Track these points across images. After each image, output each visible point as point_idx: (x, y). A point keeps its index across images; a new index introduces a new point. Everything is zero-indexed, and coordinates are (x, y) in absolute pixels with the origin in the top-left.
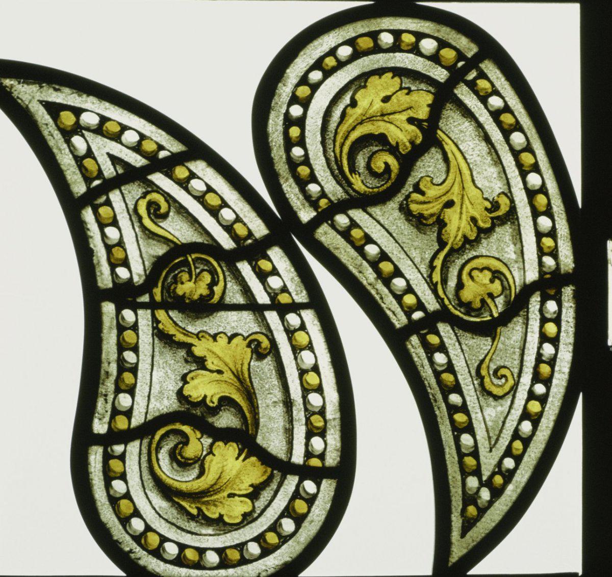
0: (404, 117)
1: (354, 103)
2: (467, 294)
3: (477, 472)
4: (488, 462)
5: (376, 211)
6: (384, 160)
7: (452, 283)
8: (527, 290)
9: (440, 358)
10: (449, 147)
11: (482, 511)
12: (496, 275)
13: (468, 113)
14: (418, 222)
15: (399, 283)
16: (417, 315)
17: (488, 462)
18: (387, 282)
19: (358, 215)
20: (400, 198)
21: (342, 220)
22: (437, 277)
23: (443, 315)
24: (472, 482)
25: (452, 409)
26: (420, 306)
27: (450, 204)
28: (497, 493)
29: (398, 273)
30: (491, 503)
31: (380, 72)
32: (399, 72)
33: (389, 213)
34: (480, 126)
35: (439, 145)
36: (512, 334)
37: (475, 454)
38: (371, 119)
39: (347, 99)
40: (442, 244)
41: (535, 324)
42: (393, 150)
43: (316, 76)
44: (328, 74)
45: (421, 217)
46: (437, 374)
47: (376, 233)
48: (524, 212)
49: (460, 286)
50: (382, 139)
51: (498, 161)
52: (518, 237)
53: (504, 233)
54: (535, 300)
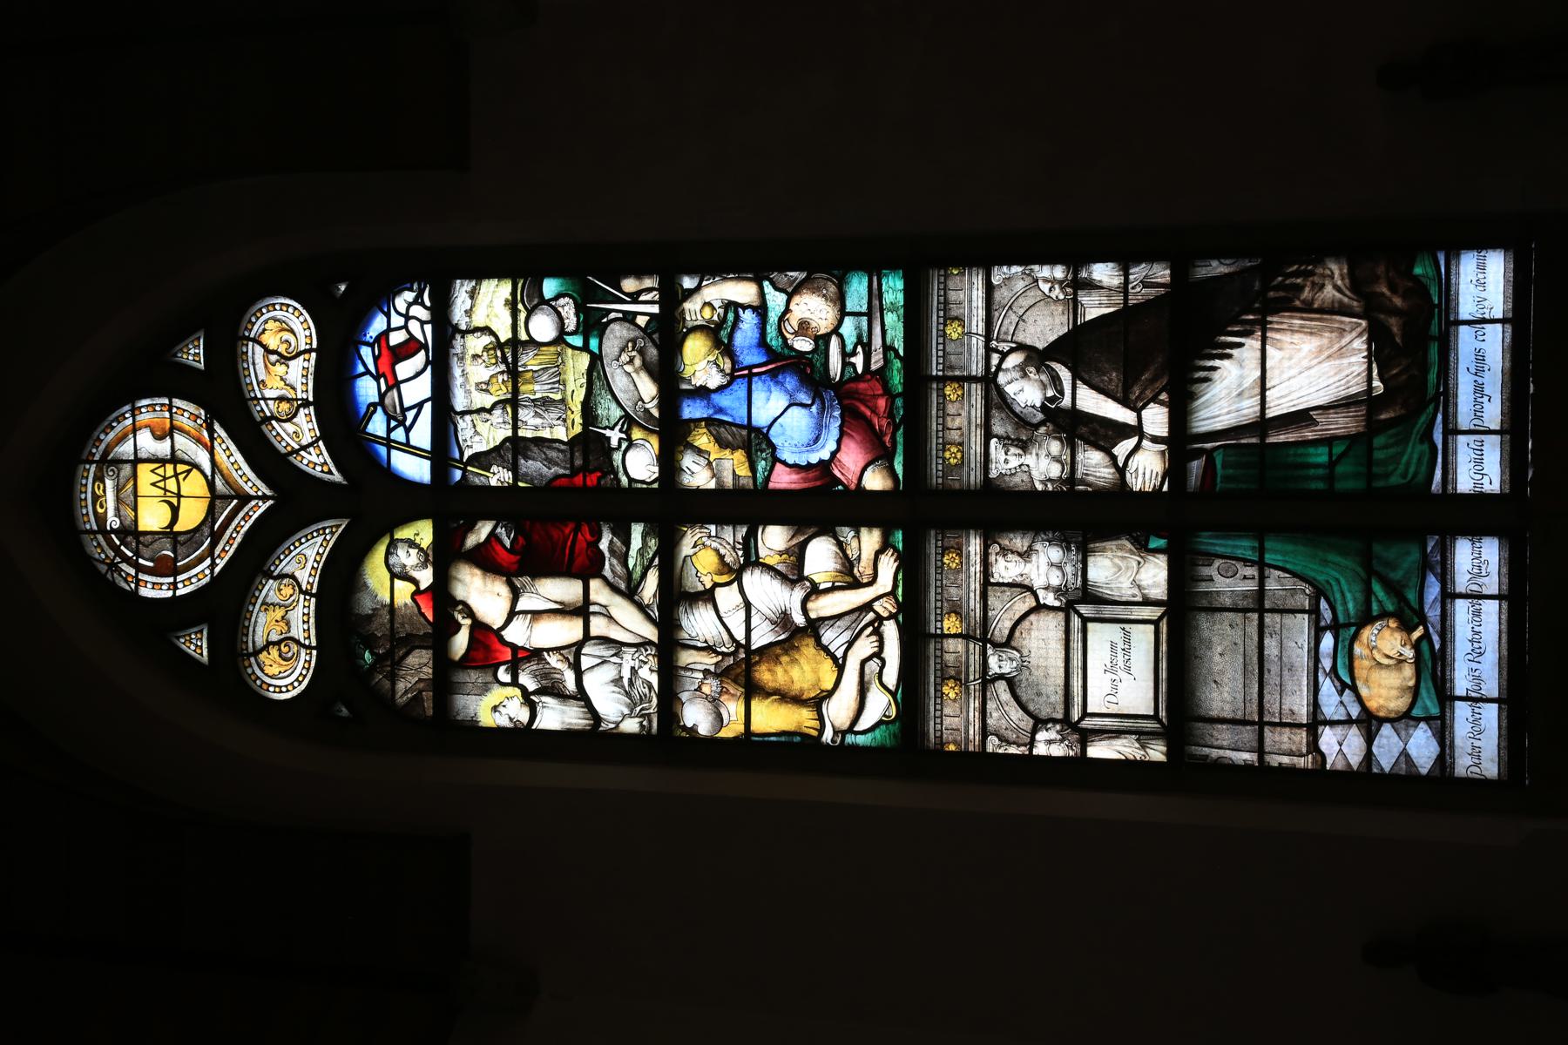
0: (270, 657)
1: (280, 672)
2: (291, 591)
3: (325, 539)
4: (320, 539)
5: (297, 637)
6: (284, 649)
7: (292, 598)
8: (275, 578)
9: (311, 581)
10: (265, 637)
11: (331, 527)
12: (280, 590)
13: (254, 642)
14: (288, 624)
15: (306, 611)
16: (308, 597)
17: (320, 539)
18: (309, 614)
19: (302, 640)
20: (288, 635)
21: (307, 643)
22: (295, 604)
23: (301, 591)
24: (328, 537)
25: (318, 563)
26: (305, 599)
27: (277, 621)
28: (324, 529)
29: (304, 614)
30: (328, 527)
31: (267, 675)
32: (262, 671)
33: (293, 633)
34: (253, 636)
35: (267, 640)
36: (288, 570)
37: (322, 545)
38: (279, 664)
39: (281, 675)
40: (287, 611)
41: (280, 567)
42: (280, 650)
43: (284, 689)
44: (280, 687)
45: (287, 625)
46: (315, 576)
47: (301, 631)
48: (260, 601)
49: (291, 596)
50: (280, 656)
51: (256, 622)
52: (267, 595)
53: (269, 600)
54: (275, 574)
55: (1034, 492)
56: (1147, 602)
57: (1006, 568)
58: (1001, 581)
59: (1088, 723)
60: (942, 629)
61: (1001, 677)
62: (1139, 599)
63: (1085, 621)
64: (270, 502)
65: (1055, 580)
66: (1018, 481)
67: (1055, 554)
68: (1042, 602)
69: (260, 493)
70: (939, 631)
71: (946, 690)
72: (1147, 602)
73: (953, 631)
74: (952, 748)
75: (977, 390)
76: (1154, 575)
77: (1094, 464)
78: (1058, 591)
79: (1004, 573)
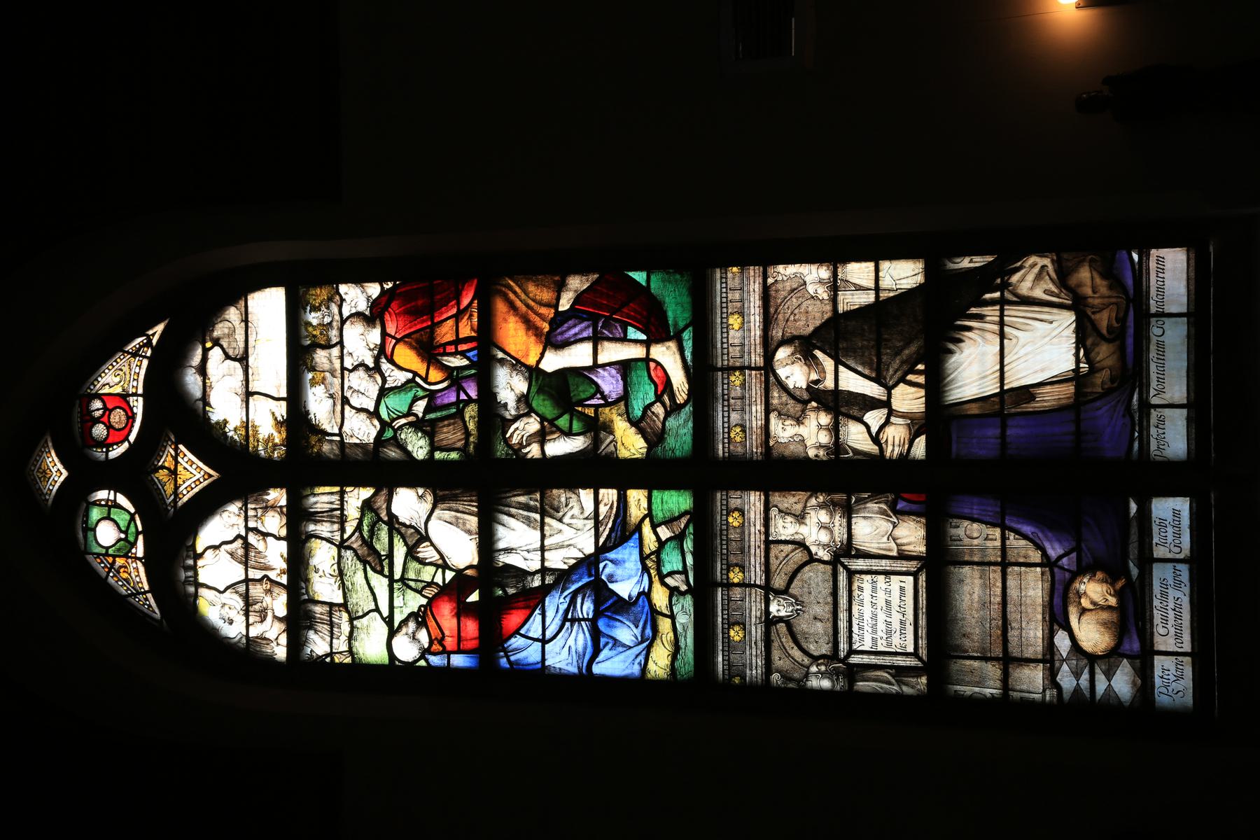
55: (807, 459)
56: (902, 556)
58: (780, 538)
59: (855, 659)
60: (728, 578)
61: (781, 619)
62: (895, 553)
63: (851, 574)
65: (824, 537)
66: (795, 449)
67: (823, 516)
70: (725, 581)
71: (732, 633)
72: (902, 556)
73: (736, 580)
74: (737, 680)
75: (755, 380)
76: (912, 534)
77: (856, 436)
78: (824, 546)
79: (782, 531)
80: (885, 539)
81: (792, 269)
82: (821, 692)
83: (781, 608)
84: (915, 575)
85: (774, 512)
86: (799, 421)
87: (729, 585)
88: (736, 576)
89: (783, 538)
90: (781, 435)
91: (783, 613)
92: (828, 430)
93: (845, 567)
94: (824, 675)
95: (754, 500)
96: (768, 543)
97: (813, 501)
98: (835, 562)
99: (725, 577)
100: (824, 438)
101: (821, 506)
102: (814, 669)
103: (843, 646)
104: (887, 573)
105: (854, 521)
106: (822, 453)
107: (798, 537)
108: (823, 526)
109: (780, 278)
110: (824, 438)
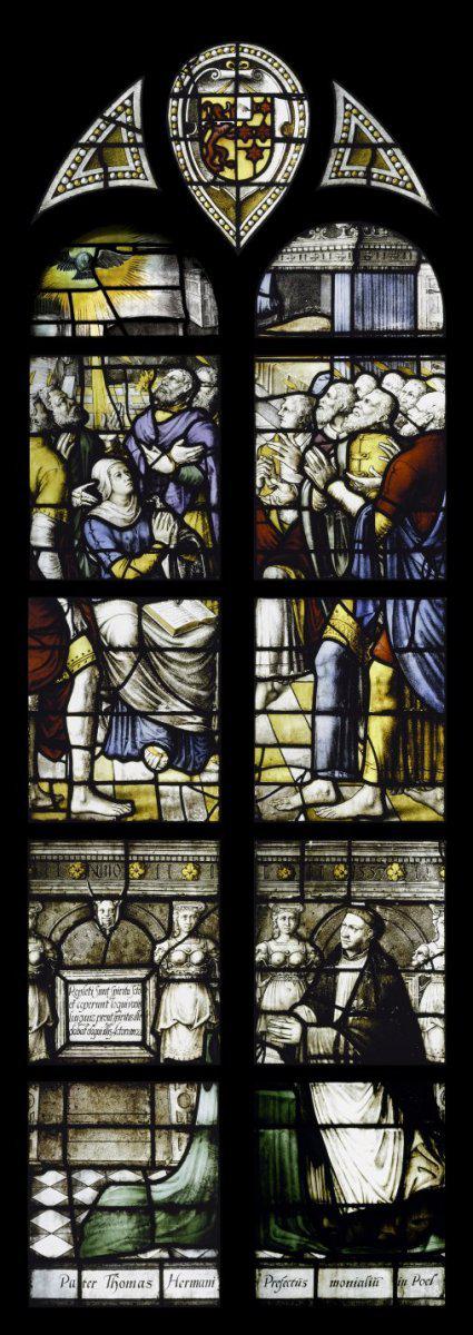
56: (159, 1037)
57: (185, 916)
59: (59, 982)
60: (133, 862)
63: (143, 981)
64: (234, 244)
67: (197, 957)
68: (158, 946)
69: (242, 233)
73: (132, 871)
76: (183, 1046)
77: (279, 993)
79: (181, 914)
80: (175, 1017)
81: (441, 929)
82: (26, 953)
83: (106, 913)
84: (142, 1044)
85: (201, 905)
86: (294, 934)
87: (127, 863)
88: (135, 870)
89: (175, 916)
90: (280, 916)
91: (100, 914)
92: (285, 962)
93: (148, 978)
94: (43, 956)
95: (208, 885)
96: (168, 900)
97: (211, 946)
98: (154, 968)
99: (135, 858)
100: (276, 958)
101: (207, 955)
102: (48, 947)
103: (70, 975)
104: (144, 1016)
105: (193, 985)
106: (259, 957)
107: (176, 928)
108: (188, 956)
109: (434, 917)
110: (276, 958)
